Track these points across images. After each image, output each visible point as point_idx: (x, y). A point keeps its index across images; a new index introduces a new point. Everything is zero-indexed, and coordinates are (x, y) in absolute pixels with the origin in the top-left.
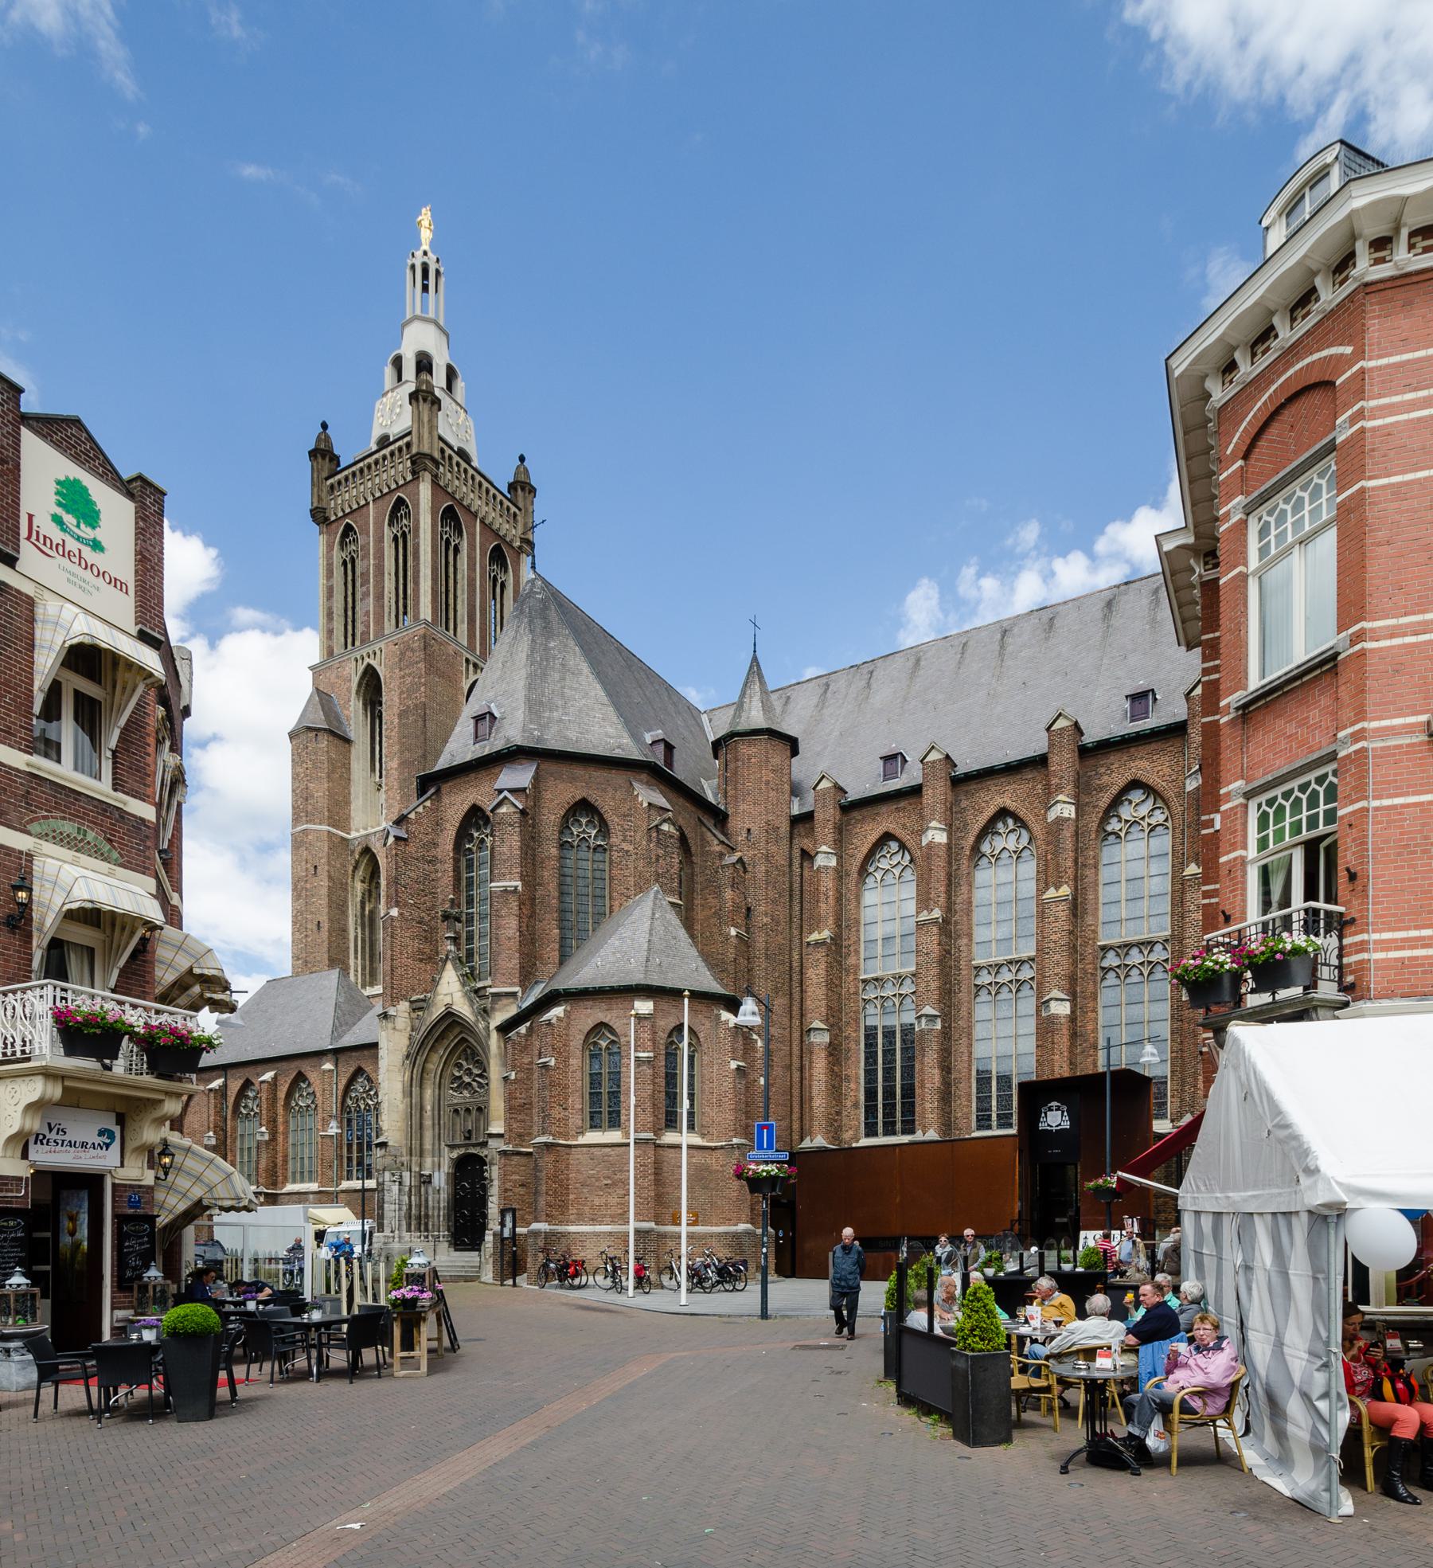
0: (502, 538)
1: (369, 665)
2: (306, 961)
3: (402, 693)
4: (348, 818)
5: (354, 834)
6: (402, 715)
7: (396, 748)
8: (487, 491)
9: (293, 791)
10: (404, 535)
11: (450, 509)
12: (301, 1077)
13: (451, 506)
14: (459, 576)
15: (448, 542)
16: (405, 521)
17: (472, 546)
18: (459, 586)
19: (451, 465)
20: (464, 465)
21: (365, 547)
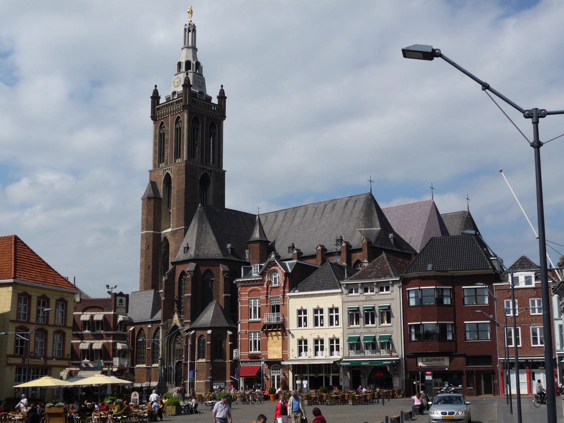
1: (168, 174)
2: (145, 280)
3: (178, 184)
6: (178, 192)
7: (175, 203)
8: (209, 105)
11: (196, 117)
12: (141, 329)
15: (194, 128)
16: (180, 123)
19: (195, 103)
21: (168, 131)
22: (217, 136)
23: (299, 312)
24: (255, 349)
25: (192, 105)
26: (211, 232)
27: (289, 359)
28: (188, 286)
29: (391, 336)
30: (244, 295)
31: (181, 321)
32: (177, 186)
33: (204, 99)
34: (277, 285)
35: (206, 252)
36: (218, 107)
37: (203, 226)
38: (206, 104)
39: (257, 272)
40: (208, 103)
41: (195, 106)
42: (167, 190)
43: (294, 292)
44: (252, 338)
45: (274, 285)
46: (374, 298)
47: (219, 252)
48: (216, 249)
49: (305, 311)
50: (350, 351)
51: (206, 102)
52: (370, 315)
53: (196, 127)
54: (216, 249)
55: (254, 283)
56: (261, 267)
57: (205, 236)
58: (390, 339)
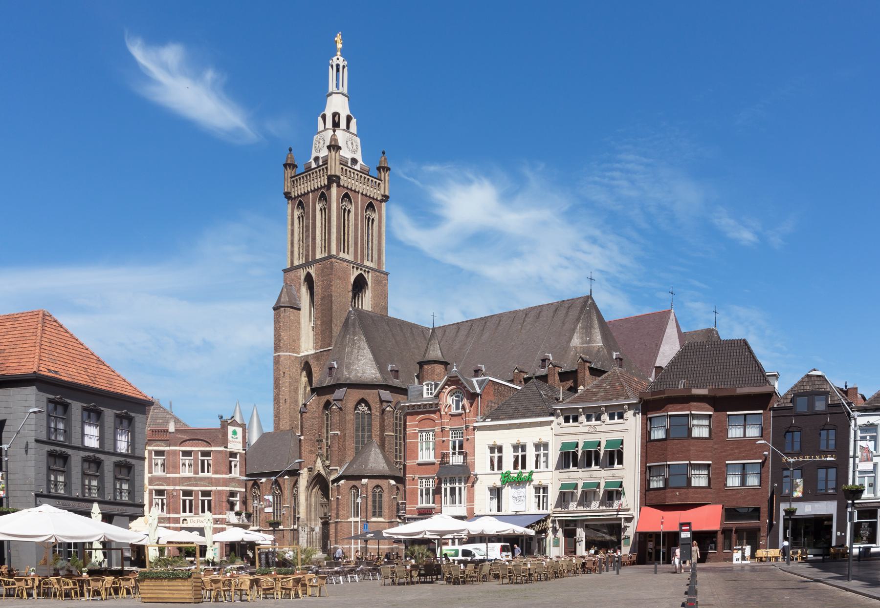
0: (373, 198)
1: (308, 272)
3: (322, 288)
4: (299, 346)
5: (302, 354)
9: (275, 336)
10: (325, 208)
13: (347, 192)
14: (350, 224)
17: (356, 208)
18: (350, 229)
19: (346, 174)
20: (352, 171)
22: (376, 223)
23: (492, 449)
24: (429, 503)
25: (342, 177)
26: (366, 346)
27: (475, 515)
28: (334, 421)
29: (622, 482)
30: (412, 426)
31: (326, 467)
32: (322, 291)
33: (359, 170)
34: (460, 411)
35: (359, 375)
36: (378, 181)
37: (356, 338)
38: (361, 176)
39: (431, 393)
40: (364, 175)
41: (345, 179)
42: (307, 292)
43: (484, 421)
44: (424, 486)
45: (454, 411)
46: (599, 429)
47: (378, 375)
48: (373, 371)
49: (500, 449)
50: (563, 503)
51: (362, 174)
52: (591, 457)
53: (347, 209)
54: (373, 371)
55: (426, 408)
56: (436, 385)
57: (358, 352)
58: (621, 486)
